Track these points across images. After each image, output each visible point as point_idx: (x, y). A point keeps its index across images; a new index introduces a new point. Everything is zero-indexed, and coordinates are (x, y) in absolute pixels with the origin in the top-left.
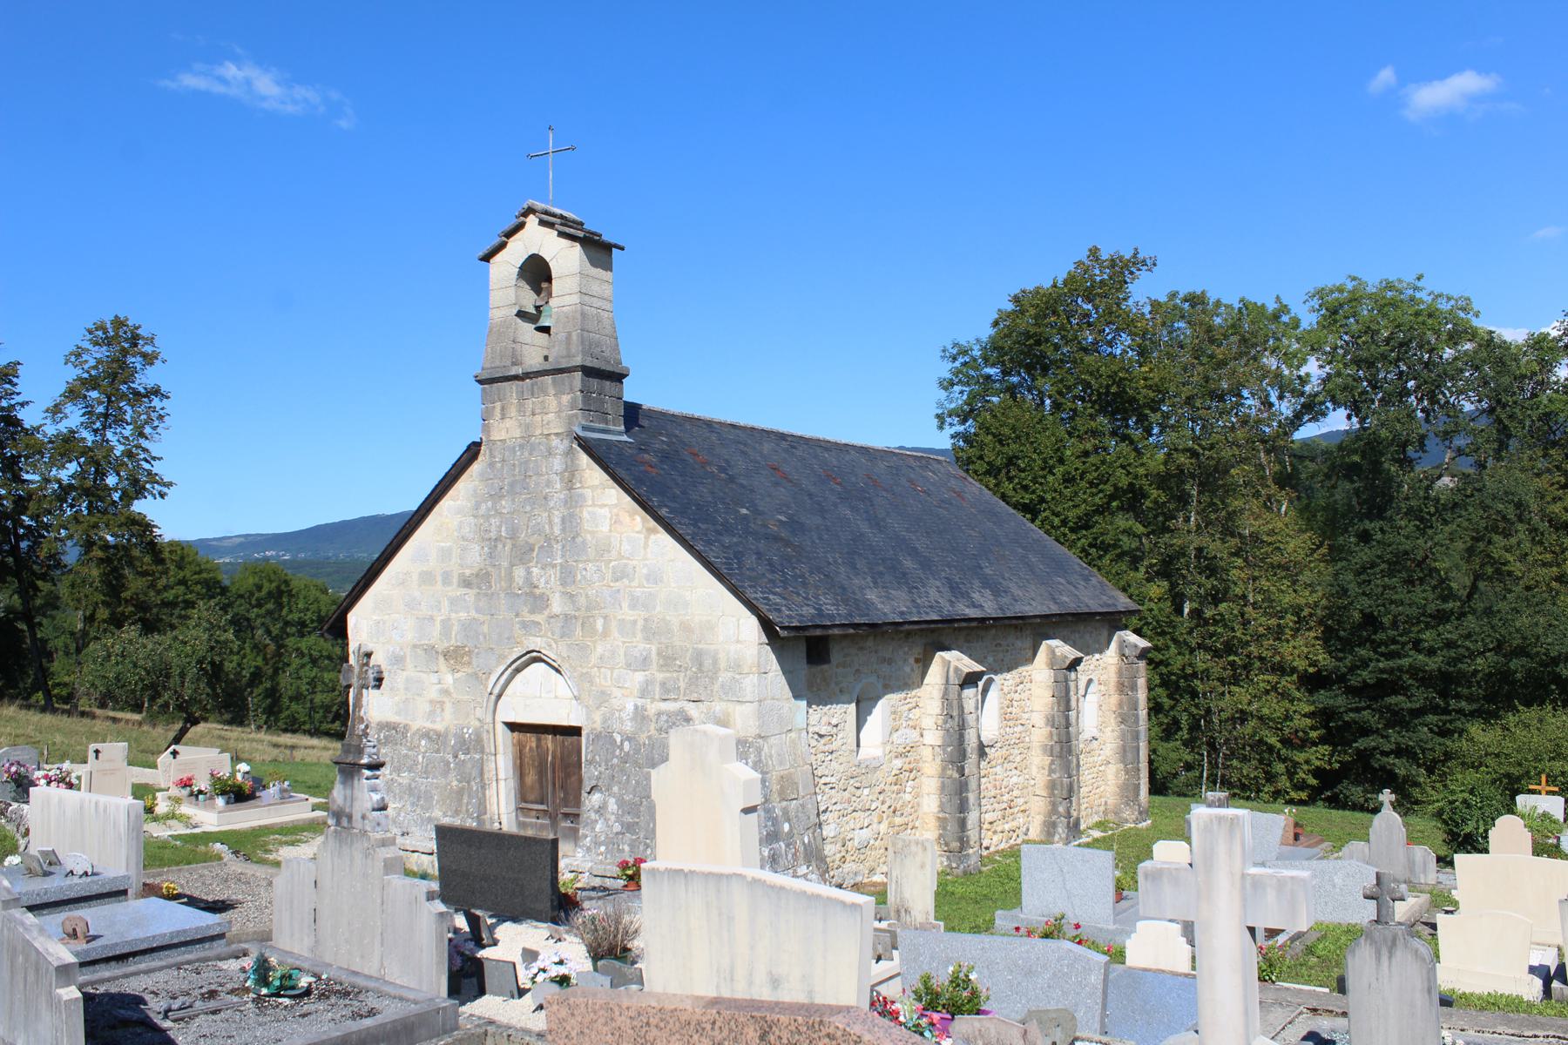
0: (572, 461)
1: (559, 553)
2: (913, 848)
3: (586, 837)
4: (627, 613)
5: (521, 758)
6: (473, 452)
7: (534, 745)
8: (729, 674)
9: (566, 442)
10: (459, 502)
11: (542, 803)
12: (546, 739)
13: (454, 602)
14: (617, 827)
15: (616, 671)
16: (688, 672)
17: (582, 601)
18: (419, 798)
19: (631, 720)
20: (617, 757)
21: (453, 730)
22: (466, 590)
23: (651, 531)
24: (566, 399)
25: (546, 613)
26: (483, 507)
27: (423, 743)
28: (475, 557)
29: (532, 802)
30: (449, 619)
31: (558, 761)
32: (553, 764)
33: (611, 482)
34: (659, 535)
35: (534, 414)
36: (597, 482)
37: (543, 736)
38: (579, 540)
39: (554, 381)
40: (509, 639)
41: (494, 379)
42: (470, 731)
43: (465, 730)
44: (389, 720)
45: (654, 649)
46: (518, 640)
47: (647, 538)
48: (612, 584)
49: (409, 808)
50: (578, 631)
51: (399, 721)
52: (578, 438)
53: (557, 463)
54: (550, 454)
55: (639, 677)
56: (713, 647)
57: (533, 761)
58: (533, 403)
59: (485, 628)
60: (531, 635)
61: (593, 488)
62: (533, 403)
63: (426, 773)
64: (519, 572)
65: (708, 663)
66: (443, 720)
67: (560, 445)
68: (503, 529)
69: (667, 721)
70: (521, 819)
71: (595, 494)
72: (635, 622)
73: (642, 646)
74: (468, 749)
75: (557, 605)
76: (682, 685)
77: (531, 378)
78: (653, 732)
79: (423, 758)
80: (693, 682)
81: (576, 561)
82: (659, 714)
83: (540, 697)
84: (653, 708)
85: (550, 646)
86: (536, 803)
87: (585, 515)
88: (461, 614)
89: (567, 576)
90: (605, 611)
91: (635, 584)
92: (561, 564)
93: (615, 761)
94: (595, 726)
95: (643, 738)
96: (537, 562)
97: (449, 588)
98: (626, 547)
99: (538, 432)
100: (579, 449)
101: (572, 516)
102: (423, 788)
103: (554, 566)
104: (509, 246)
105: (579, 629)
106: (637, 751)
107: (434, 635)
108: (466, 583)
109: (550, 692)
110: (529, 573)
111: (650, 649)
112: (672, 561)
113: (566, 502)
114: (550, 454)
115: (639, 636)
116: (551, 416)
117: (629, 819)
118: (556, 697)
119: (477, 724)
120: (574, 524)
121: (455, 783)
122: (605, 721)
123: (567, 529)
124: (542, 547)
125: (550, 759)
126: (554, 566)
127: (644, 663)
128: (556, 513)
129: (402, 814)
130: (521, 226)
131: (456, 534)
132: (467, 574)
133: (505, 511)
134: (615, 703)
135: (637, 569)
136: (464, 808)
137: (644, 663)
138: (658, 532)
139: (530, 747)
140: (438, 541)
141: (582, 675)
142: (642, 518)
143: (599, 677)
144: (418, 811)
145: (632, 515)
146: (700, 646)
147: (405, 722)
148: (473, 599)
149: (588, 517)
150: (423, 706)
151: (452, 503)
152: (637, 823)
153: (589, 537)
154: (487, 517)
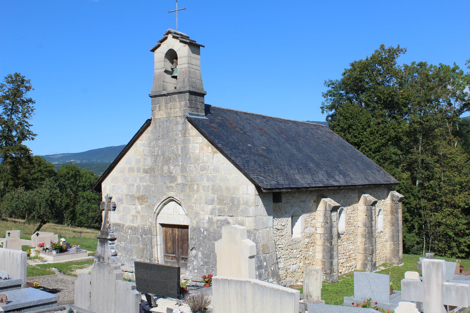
0: (185, 126)
1: (181, 160)
2: (313, 272)
3: (190, 266)
4: (206, 183)
5: (166, 237)
6: (148, 123)
7: (171, 232)
8: (244, 206)
9: (183, 119)
10: (143, 142)
11: (174, 254)
13: (141, 179)
14: (202, 263)
15: (202, 205)
17: (189, 178)
19: (207, 223)
22: (145, 174)
23: (214, 153)
24: (183, 103)
26: (152, 143)
27: (130, 231)
28: (149, 162)
29: (170, 253)
30: (139, 185)
31: (180, 238)
32: (178, 239)
33: (200, 134)
34: (218, 154)
35: (171, 109)
36: (194, 134)
37: (174, 229)
38: (188, 156)
39: (178, 97)
40: (162, 192)
41: (156, 96)
42: (147, 227)
43: (145, 226)
44: (117, 222)
45: (216, 196)
46: (165, 193)
47: (213, 155)
48: (200, 172)
49: (124, 255)
50: (188, 190)
51: (121, 223)
52: (187, 118)
53: (180, 127)
54: (177, 124)
55: (210, 207)
56: (238, 196)
57: (171, 238)
59: (153, 189)
60: (170, 191)
61: (193, 136)
63: (131, 242)
64: (166, 168)
65: (236, 202)
66: (137, 222)
67: (181, 120)
68: (160, 151)
69: (220, 224)
70: (166, 260)
72: (209, 186)
73: (211, 195)
74: (146, 233)
76: (226, 210)
77: (170, 95)
78: (215, 227)
79: (130, 237)
80: (230, 209)
81: (186, 164)
82: (218, 221)
83: (173, 214)
84: (215, 218)
86: (172, 254)
87: (190, 146)
89: (183, 169)
91: (209, 172)
92: (181, 165)
93: (201, 238)
95: (211, 230)
96: (172, 164)
98: (205, 158)
99: (173, 115)
101: (185, 147)
102: (129, 248)
103: (179, 166)
105: (188, 190)
106: (209, 235)
107: (134, 191)
108: (146, 172)
109: (177, 212)
110: (169, 168)
112: (223, 164)
113: (183, 142)
114: (177, 124)
115: (210, 191)
116: (177, 109)
117: (206, 260)
118: (179, 214)
119: (150, 224)
120: (186, 150)
121: (141, 246)
122: (197, 223)
124: (174, 158)
126: (179, 166)
127: (212, 202)
128: (179, 146)
129: (122, 258)
130: (166, 38)
131: (142, 153)
132: (146, 168)
133: (160, 145)
134: (201, 217)
135: (210, 167)
136: (145, 256)
138: (217, 153)
139: (169, 233)
140: (135, 156)
141: (189, 206)
142: (211, 148)
143: (195, 207)
145: (208, 146)
146: (233, 196)
148: (148, 178)
149: (191, 147)
152: (209, 261)
153: (192, 155)
154: (154, 147)
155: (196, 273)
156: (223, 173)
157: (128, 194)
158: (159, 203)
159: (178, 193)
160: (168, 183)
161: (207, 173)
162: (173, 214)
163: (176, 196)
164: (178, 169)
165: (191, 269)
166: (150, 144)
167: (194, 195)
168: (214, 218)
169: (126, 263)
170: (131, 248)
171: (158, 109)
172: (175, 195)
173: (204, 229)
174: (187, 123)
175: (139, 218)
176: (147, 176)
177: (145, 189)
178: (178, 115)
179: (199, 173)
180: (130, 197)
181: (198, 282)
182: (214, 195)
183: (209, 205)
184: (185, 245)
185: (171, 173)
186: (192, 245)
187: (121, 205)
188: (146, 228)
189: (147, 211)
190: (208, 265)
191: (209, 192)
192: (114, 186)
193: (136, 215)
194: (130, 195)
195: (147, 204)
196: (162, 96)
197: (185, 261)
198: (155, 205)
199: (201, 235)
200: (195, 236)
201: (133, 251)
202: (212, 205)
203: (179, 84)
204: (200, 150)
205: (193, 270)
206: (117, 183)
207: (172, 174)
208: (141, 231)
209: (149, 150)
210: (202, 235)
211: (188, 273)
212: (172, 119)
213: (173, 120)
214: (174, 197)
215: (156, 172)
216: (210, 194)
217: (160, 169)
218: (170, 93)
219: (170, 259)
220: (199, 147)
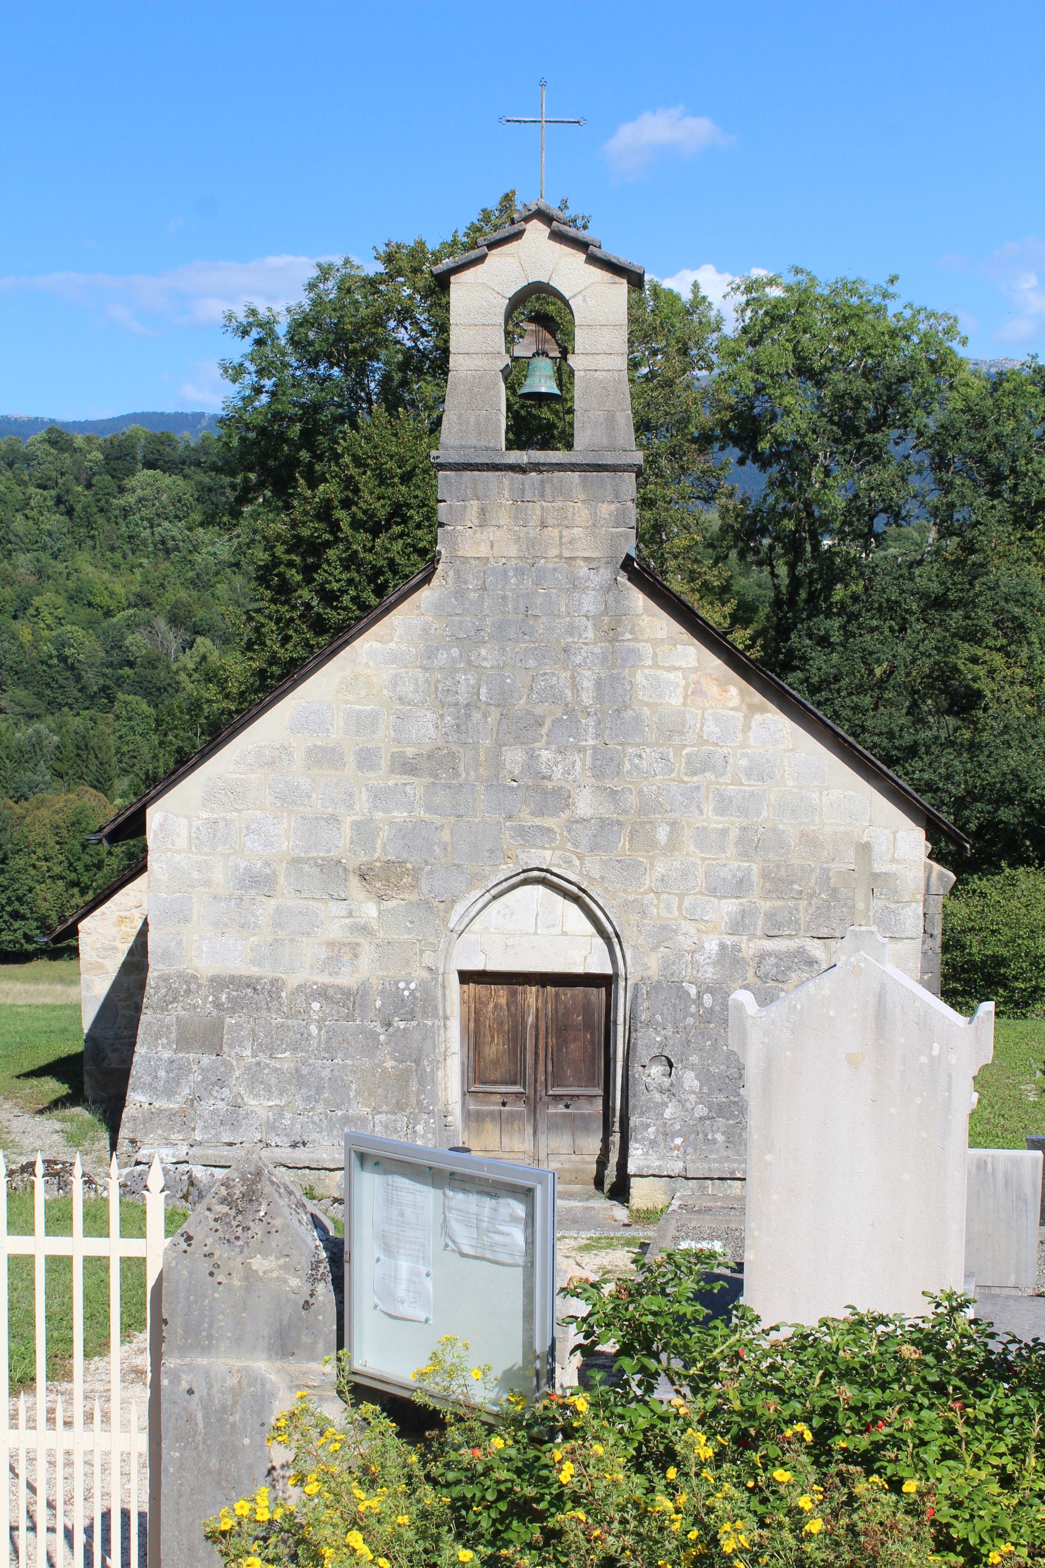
1: (591, 730)
3: (648, 1126)
5: (477, 1021)
7: (503, 1001)
9: (605, 574)
10: (392, 645)
11: (514, 1083)
12: (525, 992)
13: (379, 797)
14: (701, 1110)
15: (688, 901)
16: (814, 900)
17: (632, 799)
18: (319, 1090)
19: (715, 964)
20: (692, 1015)
21: (376, 984)
23: (753, 709)
24: (606, 510)
25: (564, 816)
26: (443, 656)
27: (316, 1006)
29: (495, 1083)
33: (686, 636)
34: (769, 715)
35: (544, 526)
36: (662, 634)
37: (520, 988)
39: (584, 481)
42: (412, 986)
44: (234, 973)
47: (748, 719)
48: (686, 779)
49: (300, 1104)
50: (624, 843)
52: (627, 564)
53: (589, 602)
54: (575, 587)
55: (729, 906)
57: (501, 1024)
58: (542, 507)
61: (655, 642)
62: (542, 507)
63: (329, 1051)
68: (483, 690)
69: (777, 966)
71: (658, 650)
72: (724, 832)
75: (585, 804)
76: (803, 917)
77: (541, 472)
79: (320, 1029)
82: (762, 957)
84: (750, 947)
85: (569, 862)
87: (639, 678)
88: (395, 814)
90: (673, 815)
91: (727, 779)
92: (594, 747)
93: (690, 1021)
94: (646, 974)
96: (548, 743)
97: (372, 775)
98: (711, 728)
99: (553, 552)
100: (629, 584)
102: (326, 1073)
103: (581, 750)
104: (487, 261)
105: (624, 843)
108: (408, 767)
109: (554, 926)
110: (532, 756)
111: (749, 870)
115: (731, 850)
118: (564, 934)
119: (425, 974)
121: (389, 1064)
122: (666, 965)
123: (607, 698)
124: (559, 720)
125: (531, 1020)
126: (581, 750)
127: (740, 886)
128: (588, 673)
129: (288, 1115)
130: (518, 235)
131: (385, 692)
135: (731, 760)
136: (413, 1100)
137: (740, 886)
138: (767, 711)
139: (496, 1006)
140: (347, 702)
141: (626, 903)
142: (742, 693)
143: (657, 906)
144: (320, 1108)
145: (723, 686)
147: (271, 975)
148: (420, 791)
149: (644, 682)
150: (311, 950)
151: (377, 645)
152: (735, 1103)
153: (646, 711)
154: (451, 671)
155: (678, 1148)
156: (791, 783)
157: (302, 855)
158: (477, 893)
159: (577, 854)
160: (529, 817)
161: (718, 783)
164: (579, 764)
166: (430, 654)
167: (652, 865)
168: (743, 946)
169: (315, 1136)
170: (336, 1073)
171: (476, 521)
172: (556, 861)
173: (698, 987)
174: (628, 589)
175: (367, 952)
176: (416, 787)
177: (404, 837)
178: (580, 554)
179: (682, 781)
180: (315, 871)
181: (711, 1179)
182: (746, 864)
183: (725, 897)
184: (572, 1046)
185: (544, 778)
186: (648, 1047)
187: (265, 899)
188: (406, 993)
189: (411, 922)
190: (732, 1113)
191: (725, 852)
192: (222, 823)
193: (348, 940)
194: (320, 862)
195: (414, 897)
196: (501, 470)
197: (567, 1106)
198: (454, 902)
199: (687, 1007)
200: (662, 1014)
201: (346, 1087)
202: (738, 897)
203: (589, 432)
204: (685, 697)
205: (661, 1137)
206: (239, 811)
207: (546, 782)
208: (378, 1004)
209: (427, 681)
210: (693, 1009)
211: (640, 1152)
212: (550, 566)
213: (555, 569)
214: (555, 870)
215: (461, 770)
216: (727, 858)
217: (482, 757)
218: (543, 464)
219: (496, 1104)
220: (683, 683)
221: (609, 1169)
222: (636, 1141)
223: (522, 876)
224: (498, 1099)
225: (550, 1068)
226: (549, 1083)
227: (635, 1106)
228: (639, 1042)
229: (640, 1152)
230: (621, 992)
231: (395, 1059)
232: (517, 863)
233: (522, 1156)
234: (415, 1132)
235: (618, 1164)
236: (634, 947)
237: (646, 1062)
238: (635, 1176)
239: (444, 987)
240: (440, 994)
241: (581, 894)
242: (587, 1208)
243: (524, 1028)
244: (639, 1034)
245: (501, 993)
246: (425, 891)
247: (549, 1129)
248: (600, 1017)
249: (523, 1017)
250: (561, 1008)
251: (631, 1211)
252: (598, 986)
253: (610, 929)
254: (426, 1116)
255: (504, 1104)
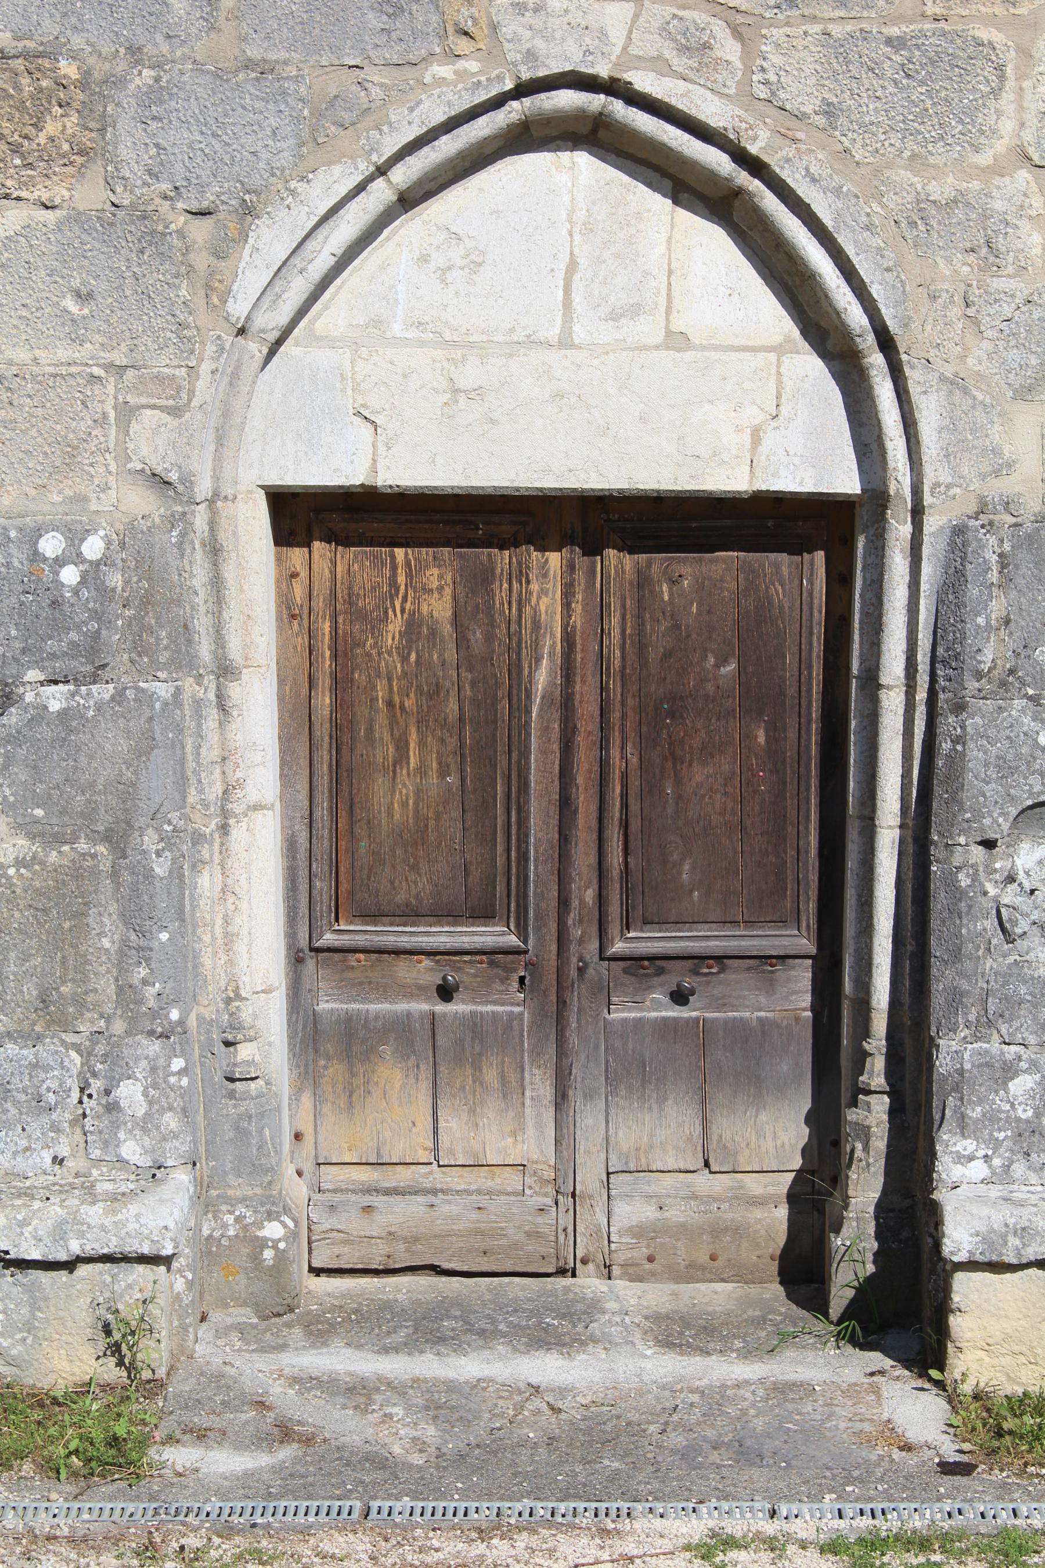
3: (1009, 1071)
5: (340, 684)
11: (484, 914)
12: (521, 573)
29: (411, 914)
31: (586, 691)
32: (567, 704)
37: (503, 559)
42: (93, 548)
57: (435, 693)
94: (997, 488)
109: (635, 311)
136: (105, 986)
139: (413, 626)
141: (923, 206)
162: (553, 331)
163: (679, 63)
165: (1025, 1113)
167: (1025, 53)
172: (648, 44)
184: (699, 774)
188: (70, 575)
189: (83, 297)
197: (680, 997)
198: (248, 212)
211: (978, 1170)
214: (644, 82)
219: (415, 991)
221: (849, 1230)
222: (963, 1127)
223: (515, 110)
224: (426, 973)
225: (615, 858)
226: (614, 909)
227: (956, 998)
228: (974, 753)
229: (978, 1170)
230: (898, 564)
231: (30, 829)
232: (494, 54)
233: (512, 1180)
234: (113, 1108)
235: (881, 1209)
236: (956, 384)
237: (997, 823)
238: (972, 1266)
239: (215, 551)
240: (200, 577)
241: (743, 178)
242: (781, 1390)
243: (520, 706)
244: (974, 723)
245: (432, 576)
246: (132, 171)
247: (612, 1080)
248: (803, 664)
249: (515, 668)
250: (659, 638)
251: (953, 1400)
252: (798, 547)
253: (856, 317)
254: (154, 1048)
255: (446, 993)
